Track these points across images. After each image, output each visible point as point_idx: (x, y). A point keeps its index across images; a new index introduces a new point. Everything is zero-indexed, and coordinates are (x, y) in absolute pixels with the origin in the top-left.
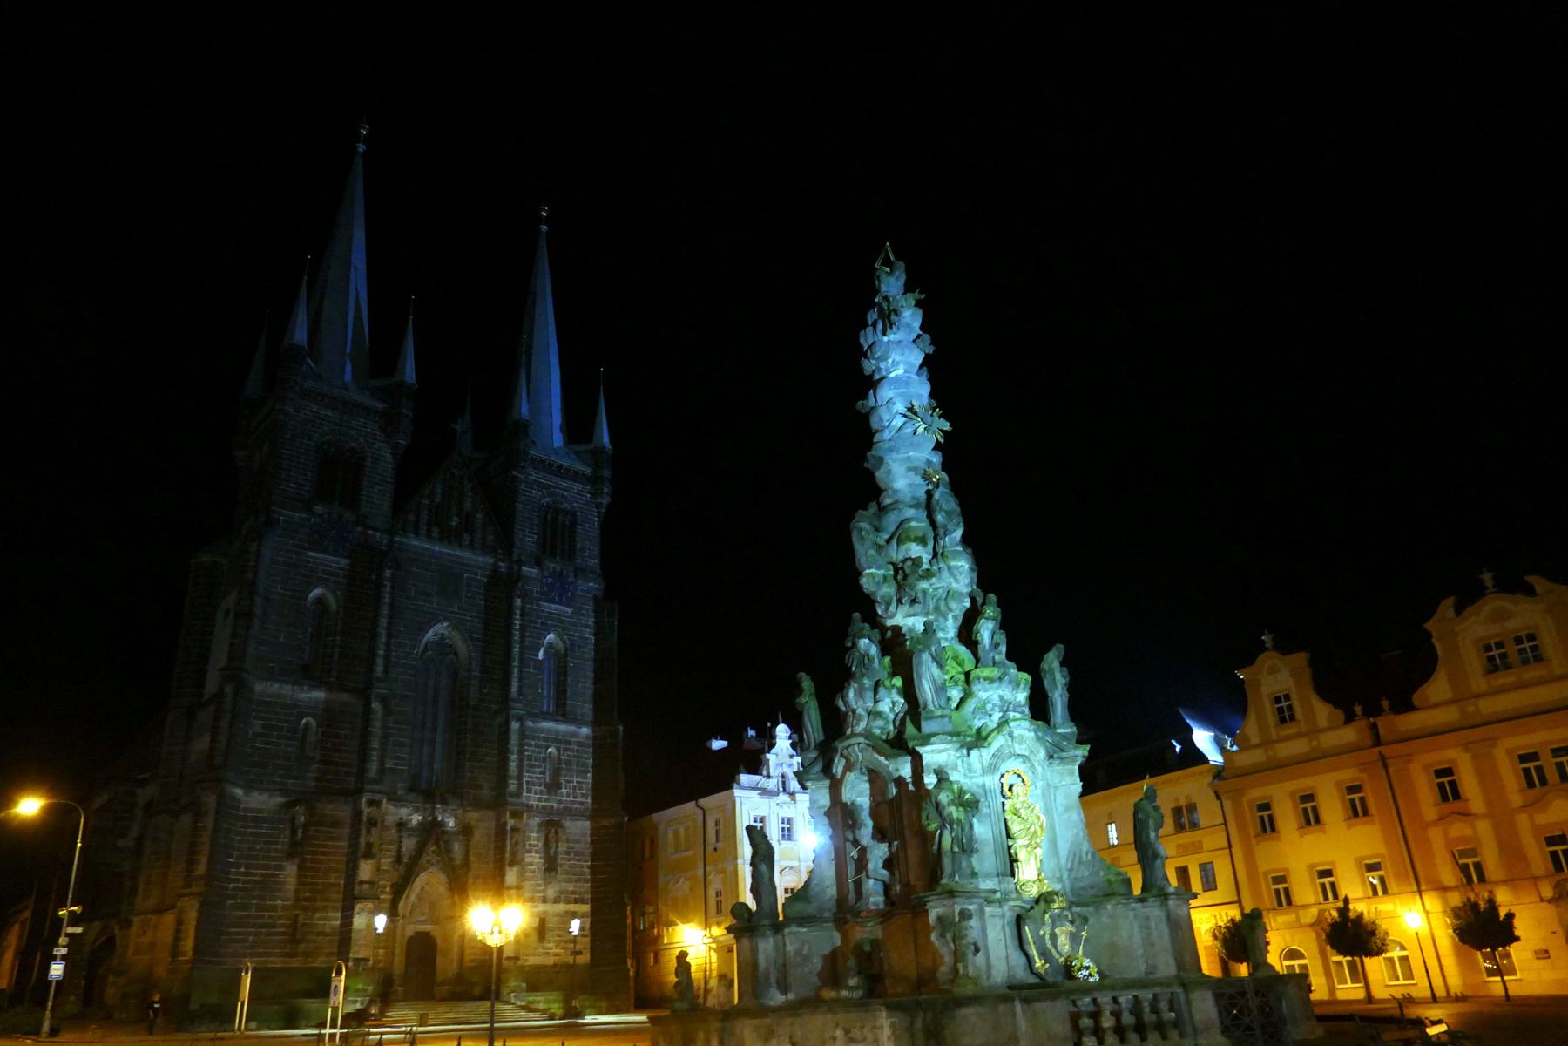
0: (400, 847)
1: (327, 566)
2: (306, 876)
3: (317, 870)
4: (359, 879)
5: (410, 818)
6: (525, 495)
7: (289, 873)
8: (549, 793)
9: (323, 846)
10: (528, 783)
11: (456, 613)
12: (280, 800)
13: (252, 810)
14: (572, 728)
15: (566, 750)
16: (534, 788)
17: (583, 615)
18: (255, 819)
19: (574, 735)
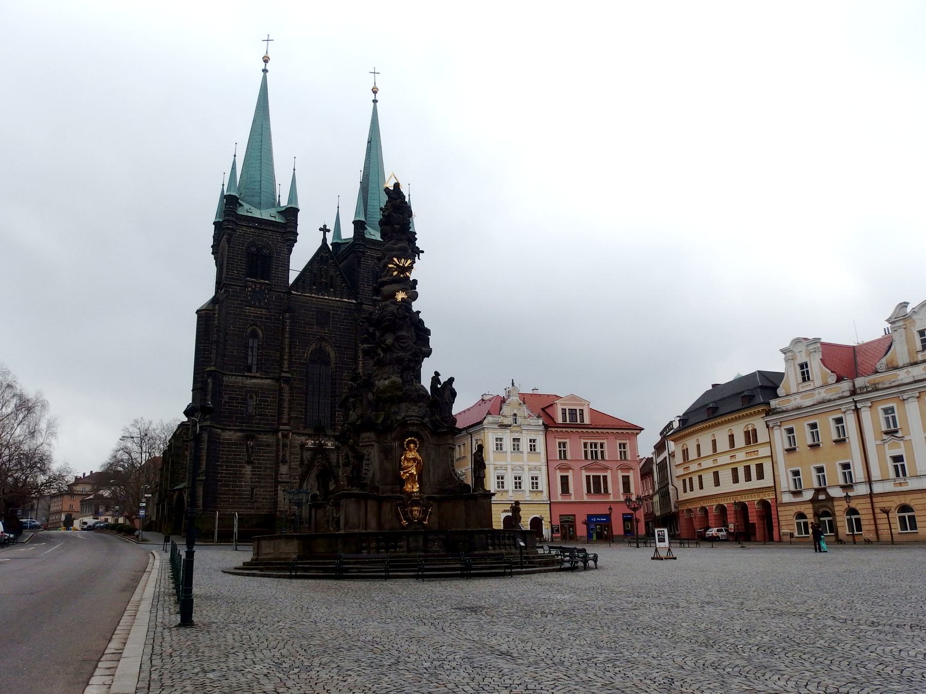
0: (302, 458)
1: (255, 313)
2: (255, 471)
3: (261, 468)
4: (280, 473)
5: (307, 442)
6: (364, 264)
7: (248, 469)
9: (263, 456)
11: (327, 333)
12: (239, 434)
13: (227, 439)
18: (228, 444)
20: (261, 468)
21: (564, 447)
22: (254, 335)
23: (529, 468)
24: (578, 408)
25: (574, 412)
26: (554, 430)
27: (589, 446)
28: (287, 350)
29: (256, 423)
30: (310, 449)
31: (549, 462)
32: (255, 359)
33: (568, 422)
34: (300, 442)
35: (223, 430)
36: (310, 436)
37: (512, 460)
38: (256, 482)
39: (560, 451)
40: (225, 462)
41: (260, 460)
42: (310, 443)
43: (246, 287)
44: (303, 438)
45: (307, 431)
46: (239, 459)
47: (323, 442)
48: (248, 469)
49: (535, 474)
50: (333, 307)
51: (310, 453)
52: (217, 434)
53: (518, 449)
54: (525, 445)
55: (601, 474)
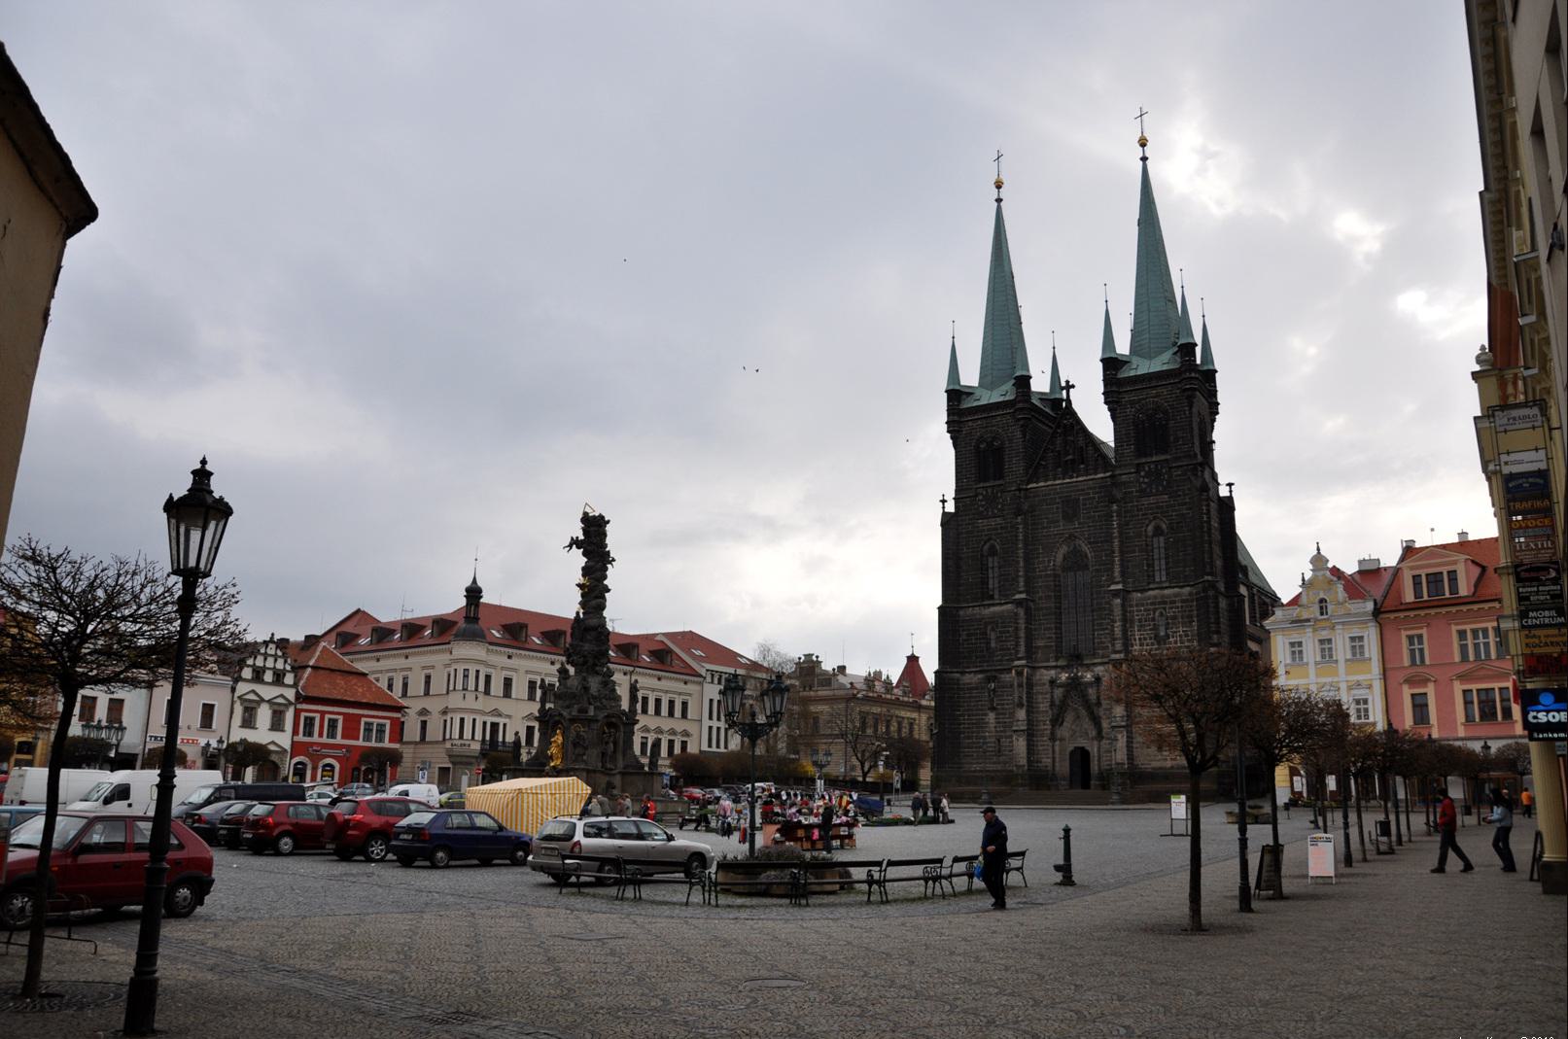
0: (1052, 697)
3: (1005, 714)
8: (1159, 643)
10: (1140, 639)
12: (980, 676)
13: (968, 684)
14: (1177, 590)
15: (1172, 608)
16: (1145, 642)
17: (1180, 496)
19: (1176, 595)
20: (1005, 714)
21: (1421, 642)
22: (993, 552)
23: (1348, 687)
24: (1445, 570)
25: (1431, 578)
26: (1392, 616)
27: (1469, 635)
28: (1022, 564)
29: (997, 661)
30: (1061, 686)
31: (1388, 673)
32: (996, 581)
33: (1426, 598)
34: (1049, 678)
35: (963, 673)
36: (1063, 668)
37: (1317, 676)
38: (1001, 731)
39: (1412, 651)
40: (968, 710)
41: (1003, 704)
42: (1064, 676)
43: (976, 496)
44: (1053, 672)
45: (1061, 663)
46: (982, 705)
47: (1080, 674)
48: (991, 716)
49: (1361, 695)
50: (1083, 490)
51: (1061, 690)
52: (953, 679)
53: (1331, 656)
54: (1342, 649)
55: (1496, 685)
